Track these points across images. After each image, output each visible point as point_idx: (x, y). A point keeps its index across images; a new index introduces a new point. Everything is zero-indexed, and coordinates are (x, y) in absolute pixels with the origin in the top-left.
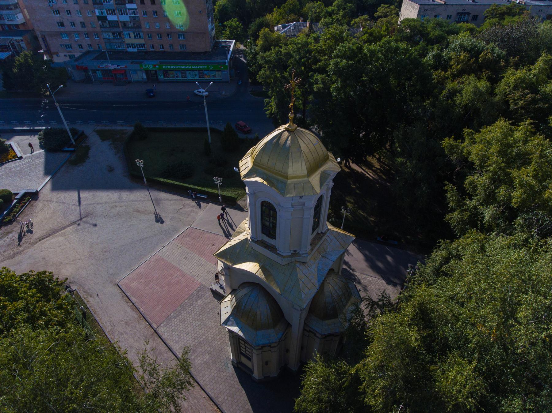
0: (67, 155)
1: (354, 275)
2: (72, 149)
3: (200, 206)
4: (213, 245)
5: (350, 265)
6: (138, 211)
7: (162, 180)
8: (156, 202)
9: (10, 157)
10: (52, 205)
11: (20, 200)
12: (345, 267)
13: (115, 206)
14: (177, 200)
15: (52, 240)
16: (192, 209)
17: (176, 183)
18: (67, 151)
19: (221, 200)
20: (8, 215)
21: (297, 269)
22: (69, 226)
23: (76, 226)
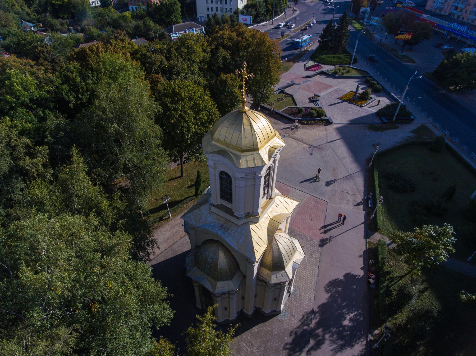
0: (380, 122)
1: (301, 351)
2: (385, 121)
3: (358, 205)
4: (311, 220)
5: (315, 350)
6: (334, 170)
7: (376, 173)
8: (349, 177)
9: (359, 103)
10: (324, 133)
11: (322, 120)
12: (312, 342)
13: (334, 158)
14: (358, 189)
15: (294, 142)
16: (351, 200)
17: (377, 183)
18: (382, 120)
19: (371, 218)
20: (307, 121)
21: (205, 206)
22: (307, 144)
23: (308, 146)
